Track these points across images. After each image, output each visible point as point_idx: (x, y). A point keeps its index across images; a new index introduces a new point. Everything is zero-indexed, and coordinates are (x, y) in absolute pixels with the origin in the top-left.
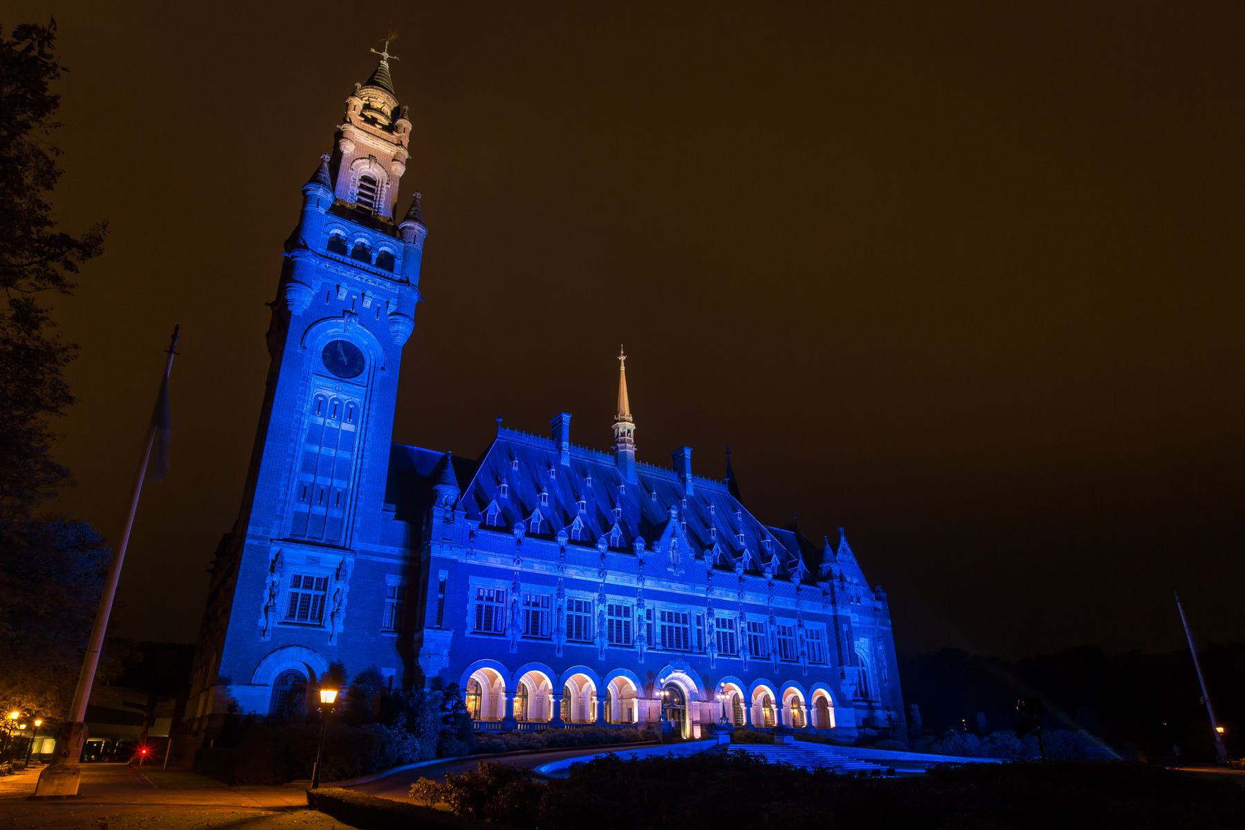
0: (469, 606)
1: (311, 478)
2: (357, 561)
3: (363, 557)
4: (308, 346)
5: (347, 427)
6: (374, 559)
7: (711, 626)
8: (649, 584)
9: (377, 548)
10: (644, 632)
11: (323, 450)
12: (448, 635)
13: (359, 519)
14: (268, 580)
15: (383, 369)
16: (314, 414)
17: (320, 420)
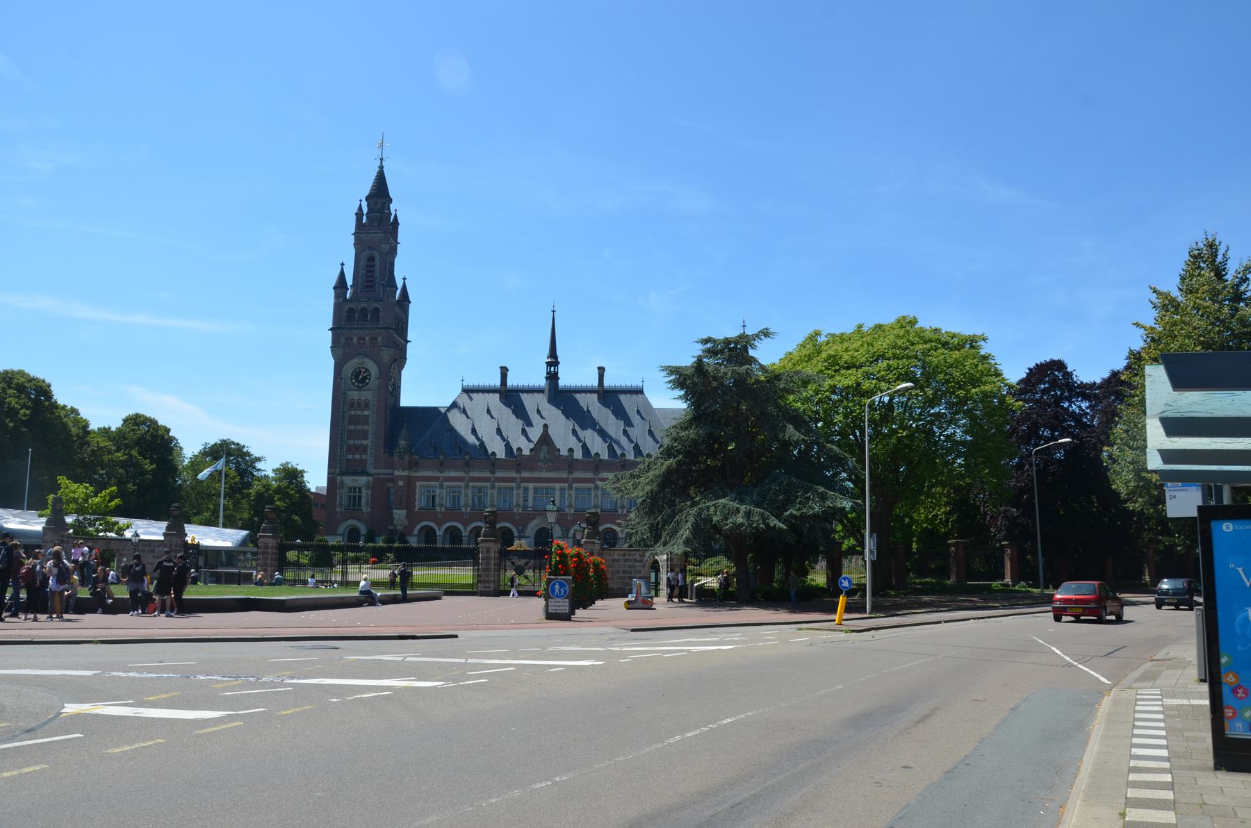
0: (417, 497)
1: (352, 442)
2: (374, 479)
3: (375, 476)
4: (343, 376)
5: (366, 413)
6: (381, 476)
7: (570, 495)
8: (525, 474)
9: (382, 471)
10: (521, 503)
11: (356, 427)
12: (405, 511)
13: (373, 459)
14: (338, 491)
15: (378, 379)
16: (349, 410)
17: (353, 413)
